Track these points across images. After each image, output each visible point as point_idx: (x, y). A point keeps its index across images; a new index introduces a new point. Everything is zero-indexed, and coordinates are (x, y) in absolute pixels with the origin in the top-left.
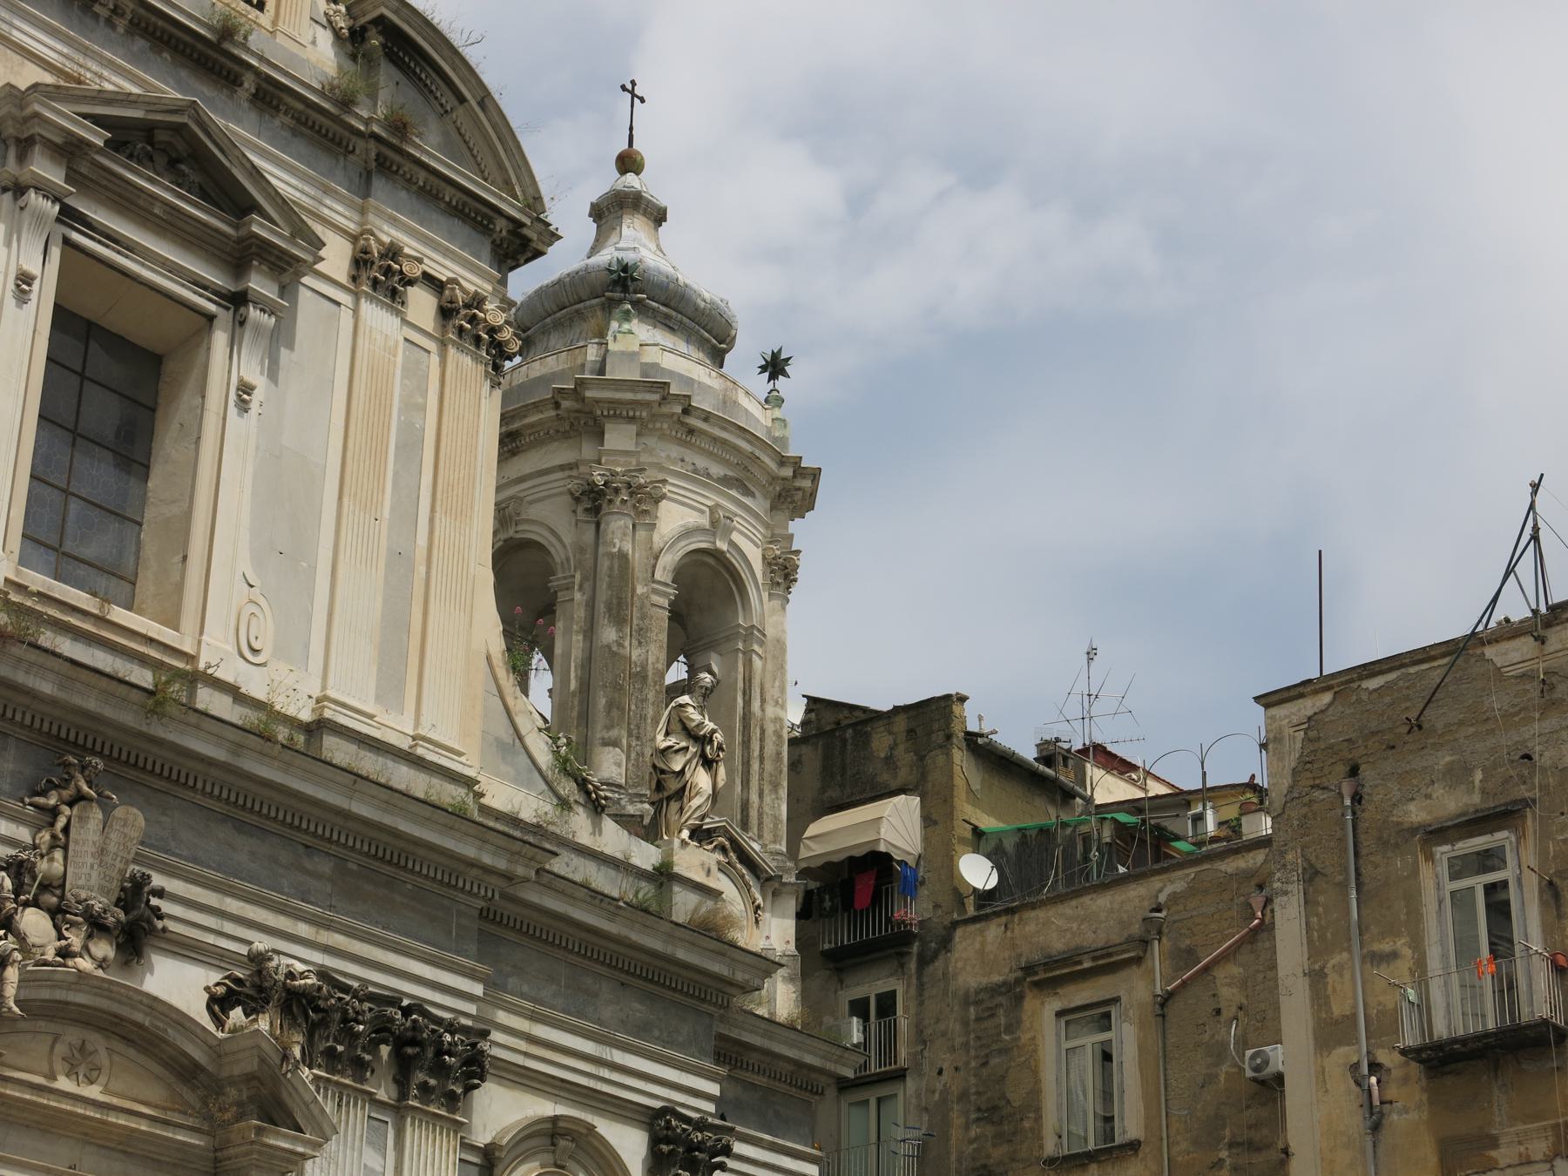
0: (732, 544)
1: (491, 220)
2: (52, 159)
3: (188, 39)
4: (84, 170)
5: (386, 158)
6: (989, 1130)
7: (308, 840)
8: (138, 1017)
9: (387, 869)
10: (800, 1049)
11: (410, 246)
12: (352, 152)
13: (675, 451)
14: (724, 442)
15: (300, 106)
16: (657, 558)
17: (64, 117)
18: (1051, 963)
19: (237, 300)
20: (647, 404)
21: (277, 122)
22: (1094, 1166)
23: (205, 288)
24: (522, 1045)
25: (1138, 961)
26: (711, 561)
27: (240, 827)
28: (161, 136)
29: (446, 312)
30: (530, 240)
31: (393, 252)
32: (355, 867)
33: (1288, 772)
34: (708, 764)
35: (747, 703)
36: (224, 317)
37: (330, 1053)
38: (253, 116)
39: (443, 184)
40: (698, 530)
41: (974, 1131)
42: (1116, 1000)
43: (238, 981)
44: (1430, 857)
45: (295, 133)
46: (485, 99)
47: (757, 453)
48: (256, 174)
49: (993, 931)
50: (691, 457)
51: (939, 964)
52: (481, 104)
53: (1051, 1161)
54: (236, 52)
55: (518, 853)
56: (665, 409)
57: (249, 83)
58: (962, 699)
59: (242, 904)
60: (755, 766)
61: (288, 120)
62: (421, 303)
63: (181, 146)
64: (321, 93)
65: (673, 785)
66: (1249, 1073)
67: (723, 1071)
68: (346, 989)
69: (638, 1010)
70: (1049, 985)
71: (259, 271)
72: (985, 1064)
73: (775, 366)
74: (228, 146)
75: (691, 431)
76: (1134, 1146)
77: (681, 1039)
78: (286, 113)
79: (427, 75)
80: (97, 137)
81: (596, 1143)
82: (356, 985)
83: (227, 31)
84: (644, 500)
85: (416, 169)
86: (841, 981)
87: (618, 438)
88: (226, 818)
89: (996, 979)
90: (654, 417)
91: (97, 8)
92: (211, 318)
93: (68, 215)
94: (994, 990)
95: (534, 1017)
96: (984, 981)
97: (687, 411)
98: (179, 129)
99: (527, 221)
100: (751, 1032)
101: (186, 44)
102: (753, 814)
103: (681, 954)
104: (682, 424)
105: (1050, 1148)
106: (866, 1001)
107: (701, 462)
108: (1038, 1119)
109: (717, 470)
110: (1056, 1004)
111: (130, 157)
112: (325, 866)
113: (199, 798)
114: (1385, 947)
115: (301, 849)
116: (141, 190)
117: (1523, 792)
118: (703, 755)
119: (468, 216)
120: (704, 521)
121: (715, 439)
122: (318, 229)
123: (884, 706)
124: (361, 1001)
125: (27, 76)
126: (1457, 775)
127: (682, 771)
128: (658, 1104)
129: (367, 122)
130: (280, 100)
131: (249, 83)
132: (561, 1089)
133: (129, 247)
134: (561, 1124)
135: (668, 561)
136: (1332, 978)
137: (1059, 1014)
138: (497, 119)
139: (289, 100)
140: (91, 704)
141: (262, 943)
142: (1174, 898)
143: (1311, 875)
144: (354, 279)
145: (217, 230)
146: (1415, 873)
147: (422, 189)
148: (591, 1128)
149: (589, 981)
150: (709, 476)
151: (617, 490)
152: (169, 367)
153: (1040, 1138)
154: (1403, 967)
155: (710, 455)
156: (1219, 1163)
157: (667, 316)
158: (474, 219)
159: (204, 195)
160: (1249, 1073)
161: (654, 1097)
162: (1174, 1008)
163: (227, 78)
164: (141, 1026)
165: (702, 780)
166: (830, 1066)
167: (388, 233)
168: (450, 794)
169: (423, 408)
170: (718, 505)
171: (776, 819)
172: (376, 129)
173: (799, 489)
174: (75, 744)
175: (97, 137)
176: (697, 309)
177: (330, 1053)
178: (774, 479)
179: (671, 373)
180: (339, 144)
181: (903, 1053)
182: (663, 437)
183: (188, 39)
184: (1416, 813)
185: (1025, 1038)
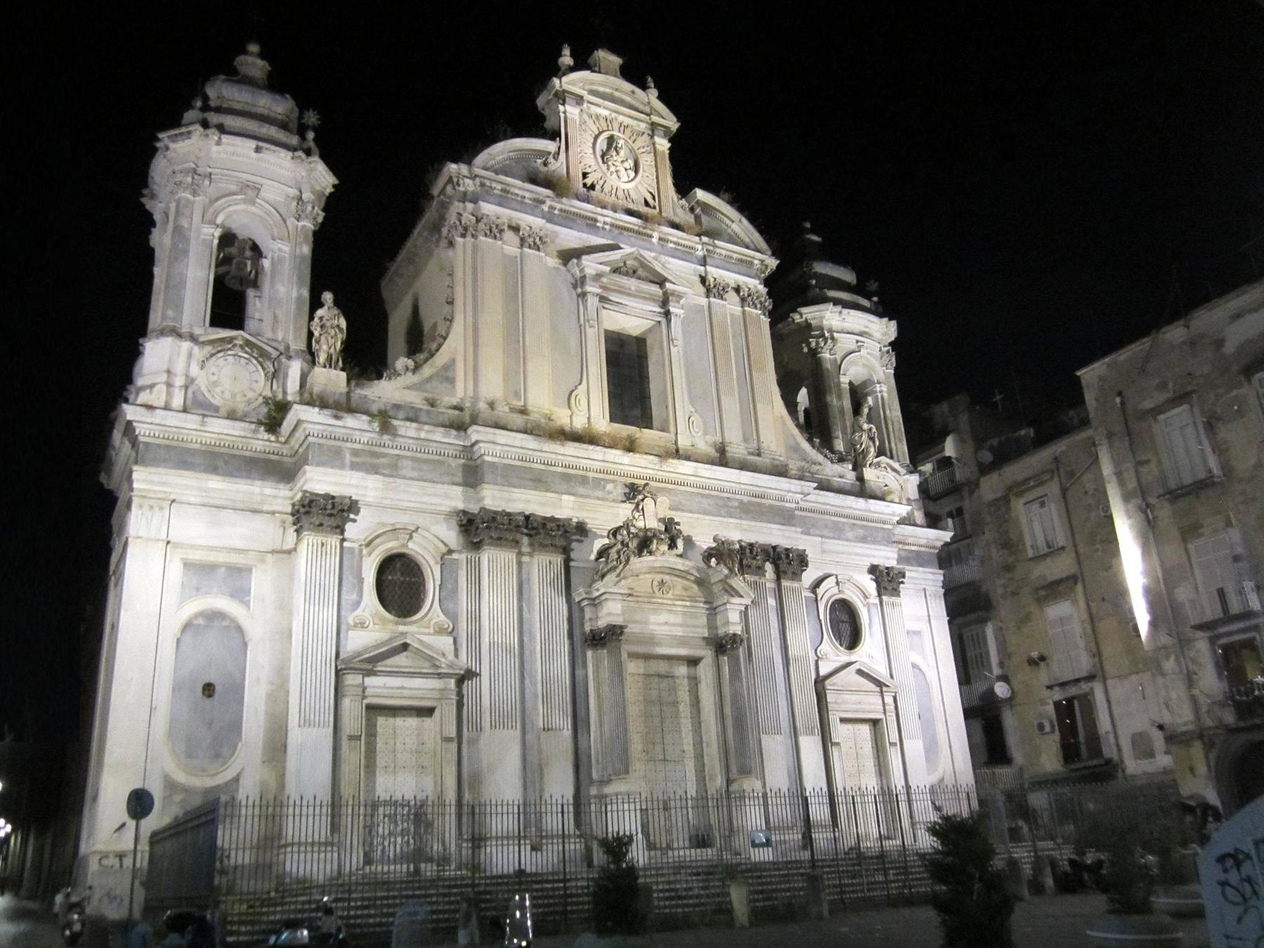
6: (1006, 552)
18: (1018, 484)
22: (1048, 560)
25: (1052, 479)
35: (884, 413)
41: (1001, 553)
42: (1046, 495)
44: (1156, 420)
49: (994, 477)
51: (976, 495)
53: (1031, 559)
60: (892, 435)
66: (1102, 514)
70: (1019, 495)
76: (1063, 548)
80: (607, 269)
89: (999, 495)
94: (998, 500)
96: (994, 497)
102: (894, 452)
105: (1030, 554)
106: (951, 512)
108: (1024, 544)
110: (1022, 501)
114: (1145, 458)
117: (1189, 388)
126: (1162, 386)
136: (1125, 475)
137: (1025, 504)
142: (1062, 452)
143: (1110, 436)
146: (1150, 427)
152: (649, 342)
153: (1026, 551)
154: (1153, 465)
156: (1097, 550)
160: (1102, 514)
162: (1069, 494)
171: (903, 453)
181: (969, 528)
184: (1148, 404)
185: (1013, 515)
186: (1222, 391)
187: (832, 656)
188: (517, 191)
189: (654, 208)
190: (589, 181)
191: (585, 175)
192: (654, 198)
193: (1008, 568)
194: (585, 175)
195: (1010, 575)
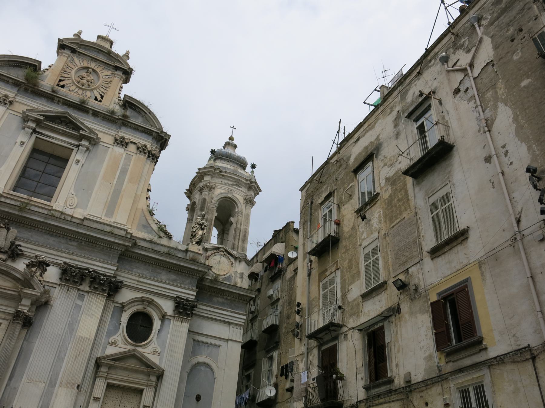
0: (233, 195)
1: (151, 133)
2: (33, 123)
3: (76, 105)
4: (43, 125)
5: (124, 123)
7: (70, 238)
8: (3, 268)
9: (93, 244)
10: (238, 291)
11: (127, 137)
12: (117, 123)
13: (220, 180)
14: (231, 177)
15: (103, 115)
16: (213, 199)
17: (34, 115)
19: (78, 146)
20: (211, 171)
21: (99, 119)
23: (72, 144)
24: (136, 283)
26: (229, 199)
27: (51, 235)
28: (62, 119)
29: (138, 148)
30: (162, 137)
31: (123, 138)
32: (84, 244)
33: (303, 202)
34: (203, 229)
36: (75, 149)
37: (66, 279)
38: (93, 118)
39: (138, 127)
40: (225, 193)
41: (288, 308)
43: (32, 262)
45: (103, 120)
46: (150, 112)
47: (239, 179)
48: (82, 123)
50: (223, 181)
52: (150, 113)
54: (86, 106)
55: (125, 240)
56: (216, 172)
57: (91, 112)
58: (294, 222)
59: (47, 249)
61: (101, 118)
62: (132, 148)
63: (67, 121)
64: (107, 112)
65: (194, 234)
67: (197, 290)
68: (73, 267)
69: (173, 277)
71: (83, 140)
72: (289, 293)
73: (253, 166)
74: (76, 119)
75: (223, 176)
77: (186, 283)
78: (101, 117)
79: (141, 111)
81: (155, 303)
82: (75, 265)
83: (83, 102)
84: (211, 188)
85: (132, 124)
86: (273, 283)
87: (207, 178)
88: (48, 234)
89: (292, 275)
90: (214, 174)
91: (55, 101)
92: (73, 149)
93: (34, 131)
94: (291, 278)
95: (140, 277)
97: (221, 172)
98: (66, 117)
99: (160, 132)
100: (222, 286)
101: (75, 106)
103: (182, 264)
104: (221, 174)
107: (226, 182)
109: (230, 183)
111: (56, 123)
112: (75, 244)
113: (40, 230)
115: (69, 240)
116: (56, 128)
118: (201, 228)
119: (146, 132)
120: (227, 192)
121: (229, 177)
122: (96, 132)
123: (281, 228)
124: (75, 269)
125: (24, 108)
127: (195, 231)
128: (175, 296)
129: (118, 116)
130: (98, 114)
131: (91, 112)
132: (148, 292)
133: (53, 138)
134: (143, 299)
135: (215, 199)
138: (153, 115)
139: (100, 114)
140: (6, 210)
141: (37, 253)
144: (114, 143)
145: (75, 134)
147: (134, 128)
148: (153, 300)
149: (159, 271)
150: (228, 184)
151: (204, 187)
155: (229, 180)
157: (227, 159)
158: (149, 133)
159: (74, 129)
161: (174, 294)
163: (86, 111)
164: (4, 270)
165: (200, 233)
166: (248, 295)
167: (121, 134)
168: (123, 233)
169: (129, 165)
170: (229, 189)
172: (119, 117)
173: (253, 186)
174: (19, 222)
175: (42, 118)
176: (234, 158)
177: (66, 279)
178: (246, 184)
179: (221, 167)
180: (114, 121)
182: (217, 177)
183: (76, 105)
185: (295, 285)
186: (346, 185)
187: (121, 344)
188: (4, 78)
189: (100, 101)
190: (61, 84)
191: (60, 81)
192: (102, 97)
193: (288, 317)
194: (60, 81)
195: (288, 321)
